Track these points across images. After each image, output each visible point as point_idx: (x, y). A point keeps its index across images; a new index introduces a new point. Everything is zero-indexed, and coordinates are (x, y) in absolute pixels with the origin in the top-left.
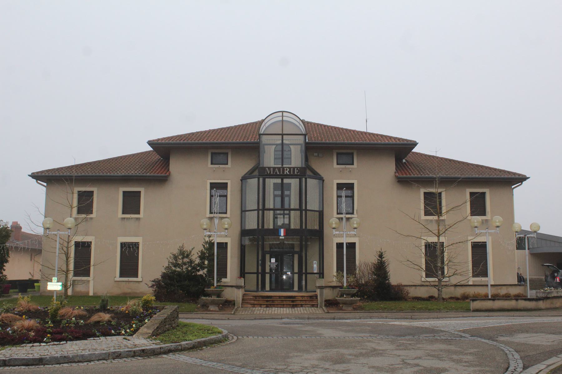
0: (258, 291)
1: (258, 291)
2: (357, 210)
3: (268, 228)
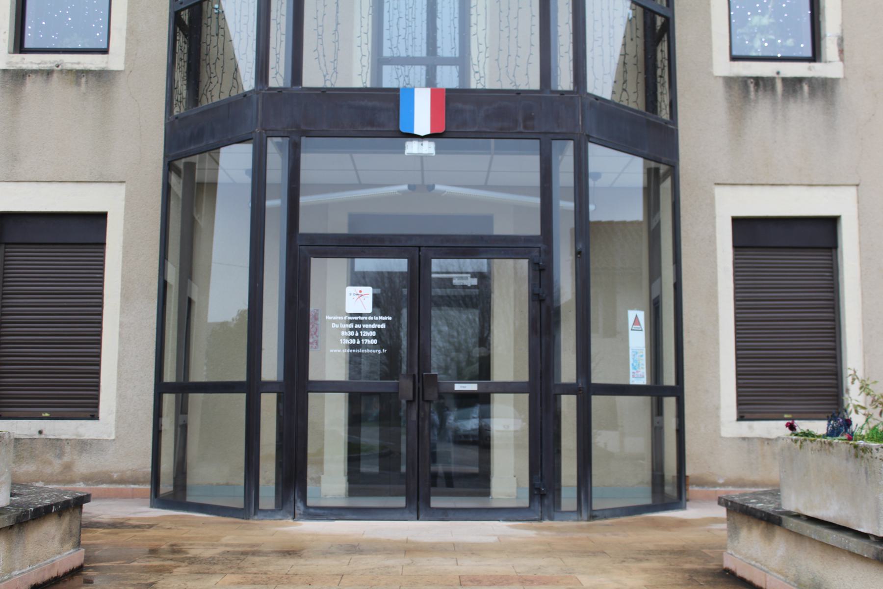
0: (257, 510)
1: (257, 510)
2: (841, 40)
3: (332, 86)
